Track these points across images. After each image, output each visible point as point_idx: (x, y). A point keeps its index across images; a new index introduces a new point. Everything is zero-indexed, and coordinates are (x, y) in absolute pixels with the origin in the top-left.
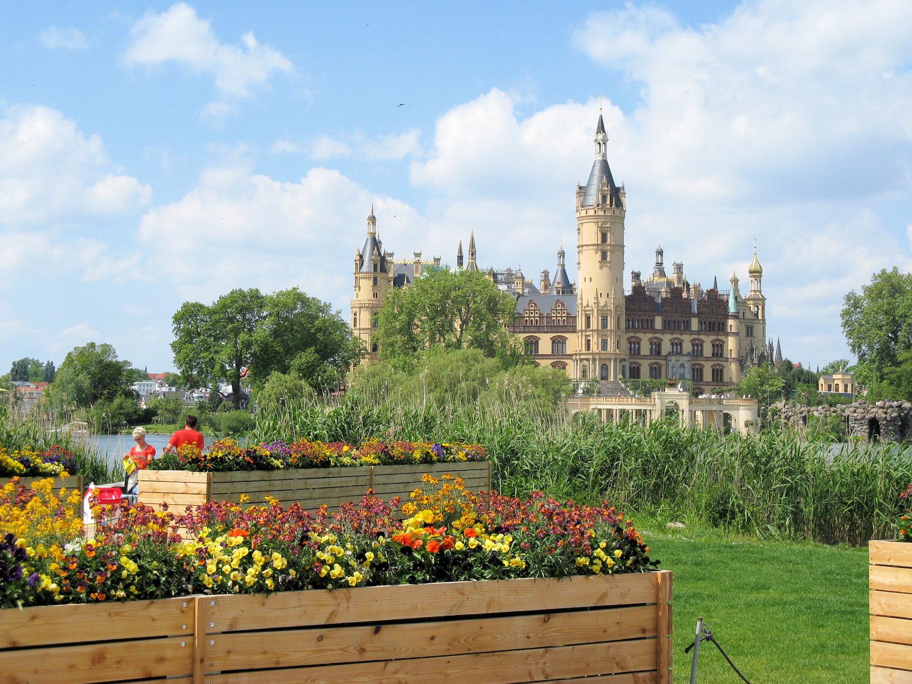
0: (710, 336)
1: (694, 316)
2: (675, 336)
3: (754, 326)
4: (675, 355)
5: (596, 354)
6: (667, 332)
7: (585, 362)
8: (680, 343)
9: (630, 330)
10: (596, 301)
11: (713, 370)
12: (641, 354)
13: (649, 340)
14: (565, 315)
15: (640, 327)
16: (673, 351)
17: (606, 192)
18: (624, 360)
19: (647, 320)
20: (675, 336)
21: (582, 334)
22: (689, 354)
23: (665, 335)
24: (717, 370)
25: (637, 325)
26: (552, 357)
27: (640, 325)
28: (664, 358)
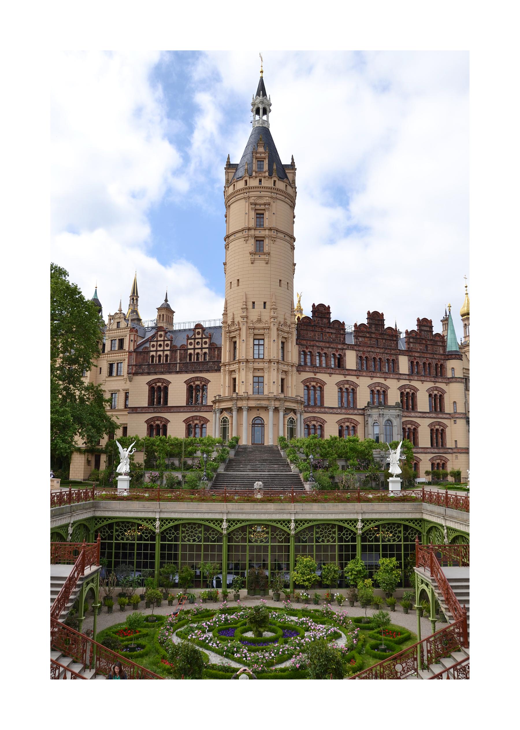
0: (425, 383)
2: (376, 380)
4: (377, 407)
5: (241, 399)
6: (364, 374)
7: (226, 414)
8: (384, 392)
9: (307, 369)
10: (245, 314)
11: (432, 430)
14: (207, 346)
15: (324, 365)
16: (373, 403)
17: (263, 155)
18: (294, 411)
19: (334, 354)
20: (376, 380)
21: (225, 371)
22: (397, 406)
23: (361, 378)
24: (437, 430)
25: (318, 361)
27: (324, 362)
28: (360, 412)
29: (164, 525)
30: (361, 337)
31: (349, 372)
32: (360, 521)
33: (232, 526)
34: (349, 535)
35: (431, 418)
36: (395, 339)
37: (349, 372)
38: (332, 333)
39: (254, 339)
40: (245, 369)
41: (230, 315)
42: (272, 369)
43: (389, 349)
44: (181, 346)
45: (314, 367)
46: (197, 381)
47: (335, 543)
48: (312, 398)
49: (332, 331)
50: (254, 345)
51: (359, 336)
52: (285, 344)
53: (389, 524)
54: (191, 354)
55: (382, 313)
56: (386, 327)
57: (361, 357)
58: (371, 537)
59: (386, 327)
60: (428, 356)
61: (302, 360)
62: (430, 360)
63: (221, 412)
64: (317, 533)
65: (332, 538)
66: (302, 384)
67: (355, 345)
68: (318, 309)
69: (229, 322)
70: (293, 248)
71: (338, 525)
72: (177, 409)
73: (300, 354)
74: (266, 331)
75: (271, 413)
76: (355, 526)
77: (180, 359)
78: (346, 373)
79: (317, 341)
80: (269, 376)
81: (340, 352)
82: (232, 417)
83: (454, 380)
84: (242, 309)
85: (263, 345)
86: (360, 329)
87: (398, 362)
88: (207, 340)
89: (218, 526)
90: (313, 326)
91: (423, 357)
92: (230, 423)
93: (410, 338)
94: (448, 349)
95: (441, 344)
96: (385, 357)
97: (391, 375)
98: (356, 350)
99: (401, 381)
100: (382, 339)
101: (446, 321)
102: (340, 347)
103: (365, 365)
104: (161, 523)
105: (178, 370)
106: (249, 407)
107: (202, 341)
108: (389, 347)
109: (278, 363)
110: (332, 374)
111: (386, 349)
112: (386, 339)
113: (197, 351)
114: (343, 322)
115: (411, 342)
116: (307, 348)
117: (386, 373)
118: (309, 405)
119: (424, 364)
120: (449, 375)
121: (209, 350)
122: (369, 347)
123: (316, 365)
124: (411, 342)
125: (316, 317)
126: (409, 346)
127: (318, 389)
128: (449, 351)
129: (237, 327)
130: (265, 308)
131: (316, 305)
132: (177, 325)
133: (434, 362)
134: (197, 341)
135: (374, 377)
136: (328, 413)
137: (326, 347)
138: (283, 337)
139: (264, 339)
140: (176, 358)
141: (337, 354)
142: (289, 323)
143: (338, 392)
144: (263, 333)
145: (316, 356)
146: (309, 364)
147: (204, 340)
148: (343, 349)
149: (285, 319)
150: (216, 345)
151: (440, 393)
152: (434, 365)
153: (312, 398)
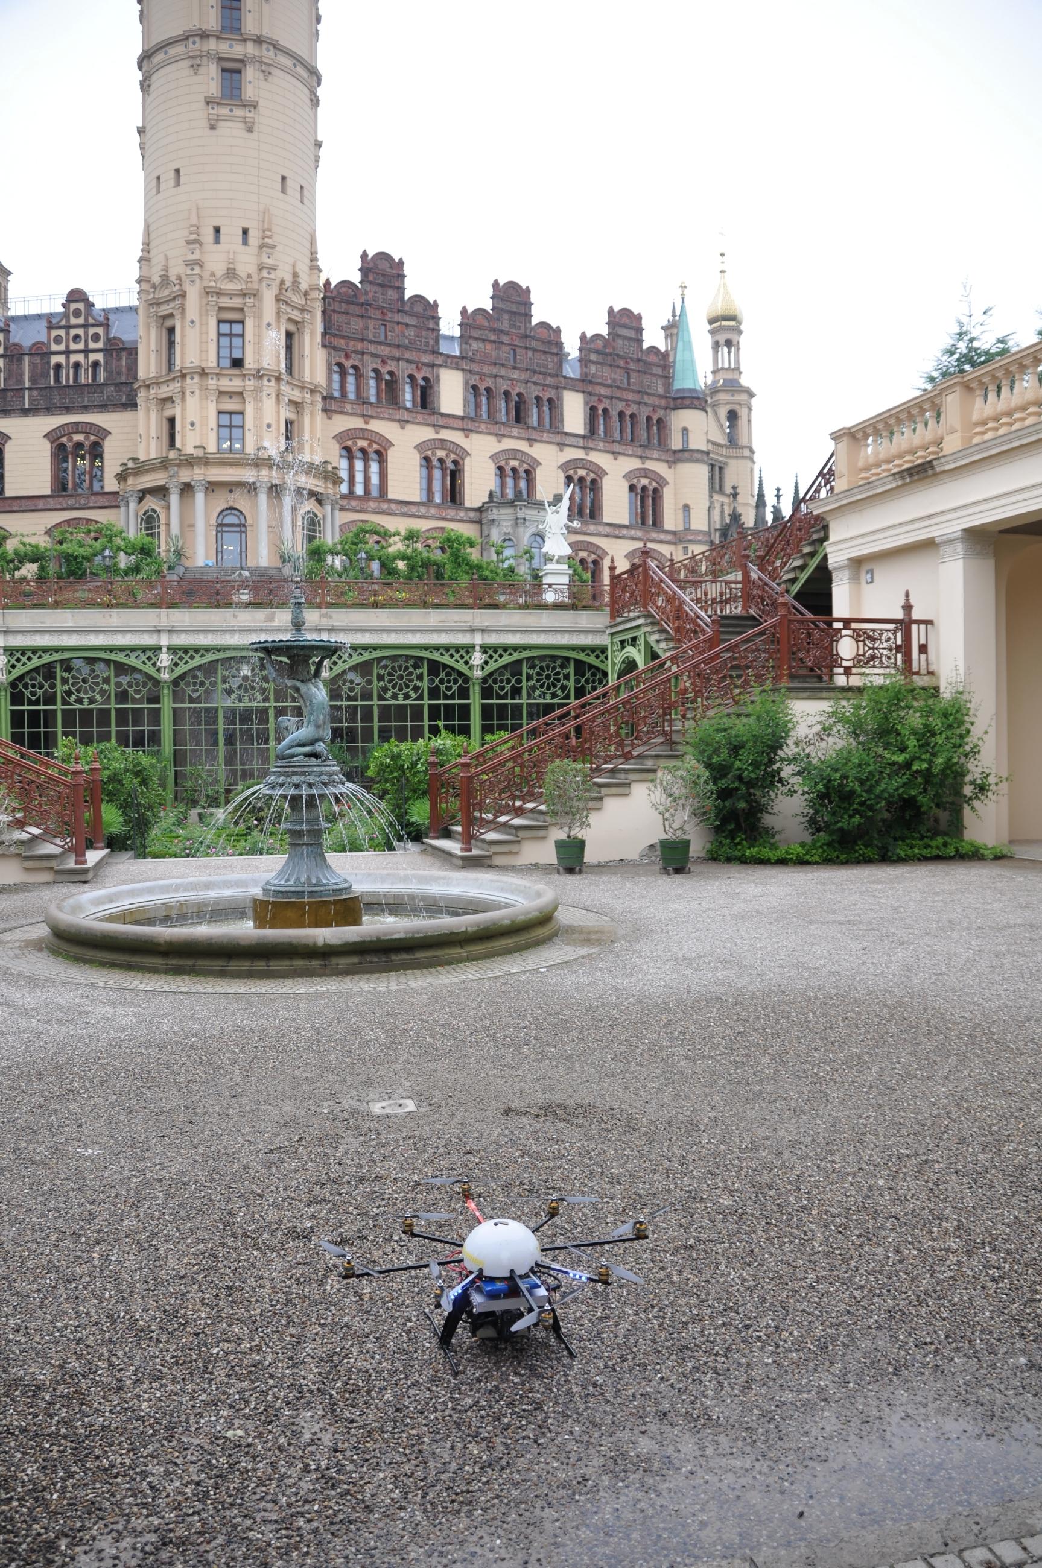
0: (621, 458)
1: (573, 385)
2: (509, 444)
3: (726, 464)
4: (511, 504)
5: (189, 462)
6: (483, 427)
7: (151, 503)
9: (348, 408)
10: (196, 256)
12: (390, 496)
13: (419, 447)
16: (503, 494)
20: (509, 444)
23: (474, 436)
26: (51, 503)
28: (472, 514)
29: (19, 665)
30: (476, 339)
31: (448, 421)
32: (478, 648)
33: (181, 663)
34: (455, 683)
35: (632, 538)
36: (555, 350)
37: (448, 421)
38: (407, 325)
39: (219, 321)
40: (197, 392)
41: (157, 260)
42: (264, 393)
43: (540, 373)
44: (34, 345)
45: (364, 403)
46: (78, 432)
47: (422, 699)
48: (359, 477)
49: (407, 320)
50: (219, 335)
51: (470, 337)
52: (296, 338)
53: (542, 658)
54: (58, 366)
55: (527, 288)
56: (535, 321)
58: (502, 688)
59: (535, 321)
60: (631, 396)
61: (336, 386)
62: (634, 408)
63: (141, 500)
64: (380, 678)
65: (416, 688)
66: (334, 441)
67: (462, 358)
68: (376, 265)
69: (156, 279)
70: (315, 102)
71: (429, 660)
72: (28, 504)
73: (330, 371)
74: (248, 300)
75: (263, 497)
76: (466, 663)
77: (31, 380)
78: (440, 423)
79: (371, 342)
80: (258, 410)
81: (426, 372)
82: (168, 508)
83: (686, 455)
84: (188, 242)
85: (242, 335)
86: (474, 320)
87: (562, 405)
88: (100, 331)
89: (149, 664)
90: (362, 304)
91: (620, 399)
92: (163, 521)
93: (590, 351)
94: (678, 385)
95: (659, 371)
96: (533, 392)
97: (545, 435)
98: (463, 370)
99: (567, 450)
100: (526, 348)
101: (673, 328)
102: (426, 359)
103: (484, 408)
104: (9, 661)
105: (27, 406)
106: (209, 482)
107: (86, 333)
108: (542, 370)
109: (278, 379)
110: (407, 422)
111: (535, 372)
112: (535, 350)
113: (74, 358)
114: (435, 302)
115: (593, 362)
116: (347, 356)
117: (534, 428)
118: (351, 491)
119: (621, 414)
120: (676, 443)
121: (105, 356)
122: (495, 364)
123: (368, 398)
124: (593, 362)
125: (371, 283)
126: (587, 370)
127: (374, 456)
128: (678, 391)
129: (177, 288)
130: (245, 242)
131: (370, 256)
132: (20, 306)
133: (643, 413)
134: (73, 332)
135: (504, 436)
136: (396, 515)
137: (393, 358)
138: (290, 320)
139: (242, 322)
140: (22, 375)
141: (419, 377)
142: (304, 286)
143: (421, 466)
144: (240, 306)
145: (368, 378)
146: (352, 396)
147: (92, 331)
148: (433, 366)
149: (295, 275)
150: (123, 343)
151: (654, 484)
152: (642, 419)
153: (359, 477)
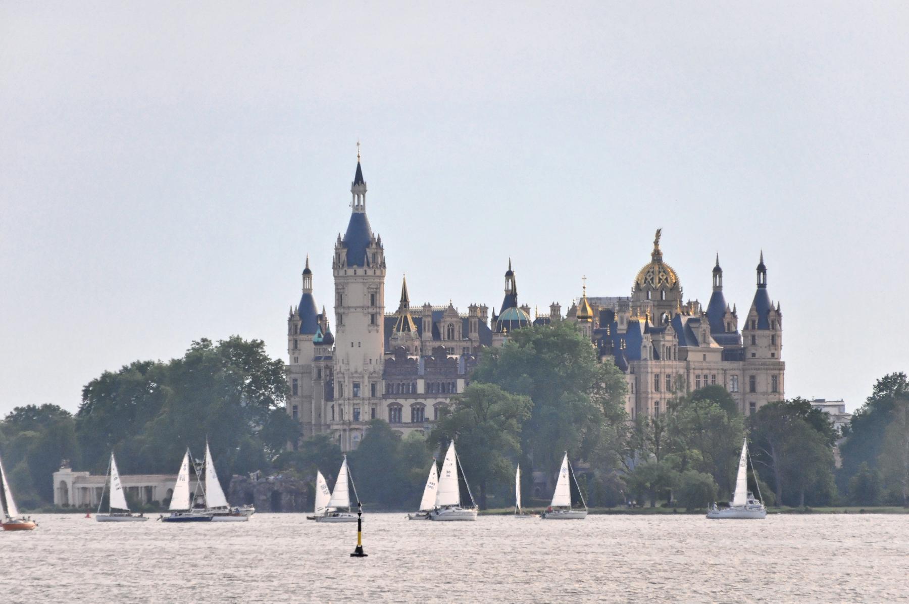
1: (461, 377)
10: (347, 368)
57: (428, 383)
